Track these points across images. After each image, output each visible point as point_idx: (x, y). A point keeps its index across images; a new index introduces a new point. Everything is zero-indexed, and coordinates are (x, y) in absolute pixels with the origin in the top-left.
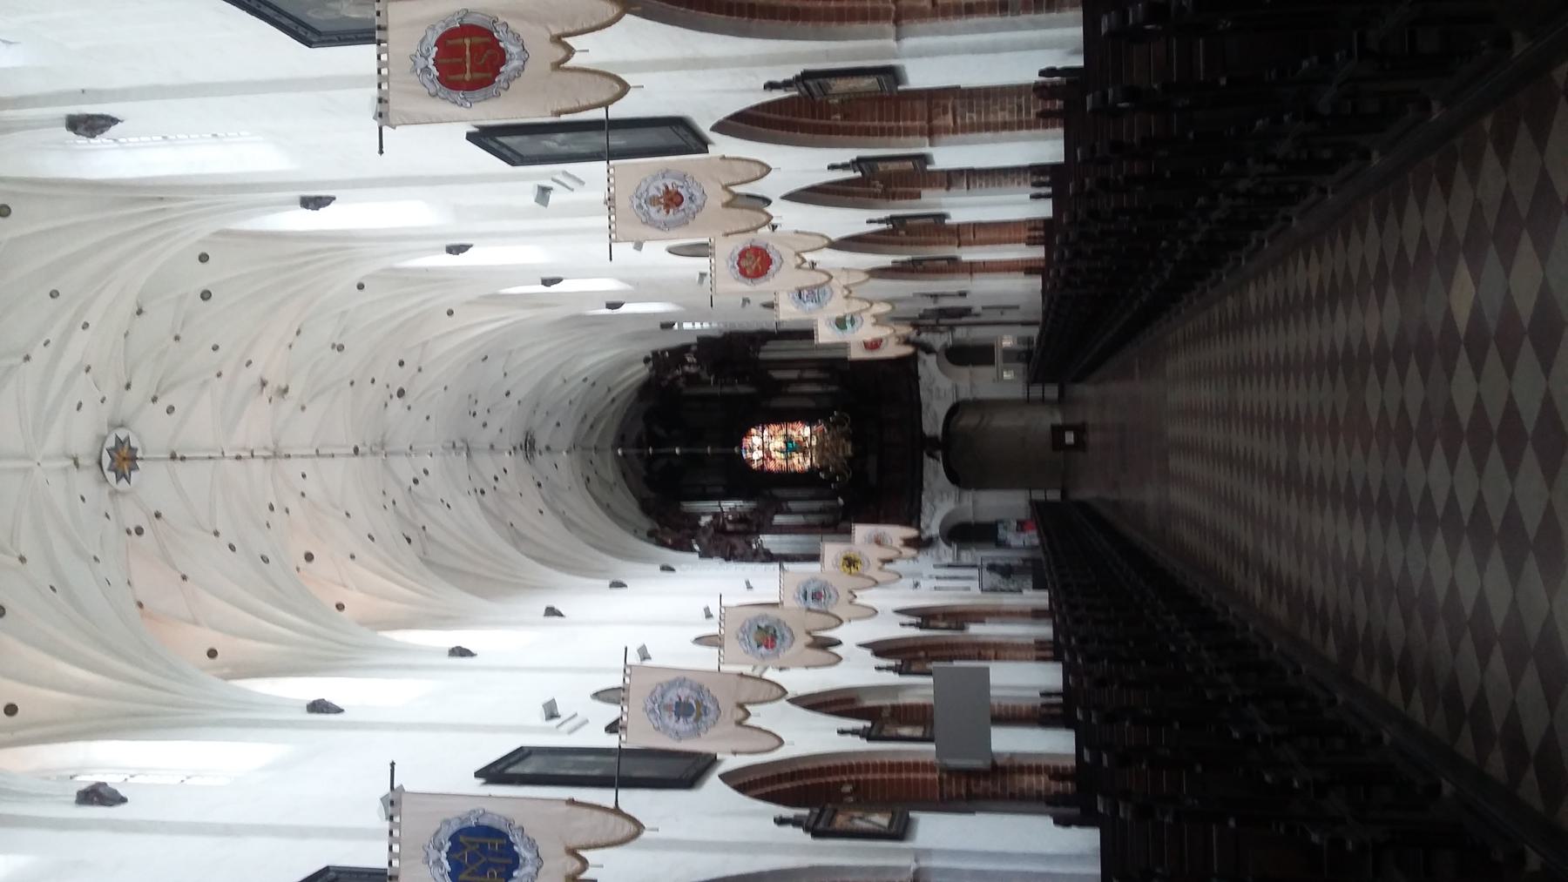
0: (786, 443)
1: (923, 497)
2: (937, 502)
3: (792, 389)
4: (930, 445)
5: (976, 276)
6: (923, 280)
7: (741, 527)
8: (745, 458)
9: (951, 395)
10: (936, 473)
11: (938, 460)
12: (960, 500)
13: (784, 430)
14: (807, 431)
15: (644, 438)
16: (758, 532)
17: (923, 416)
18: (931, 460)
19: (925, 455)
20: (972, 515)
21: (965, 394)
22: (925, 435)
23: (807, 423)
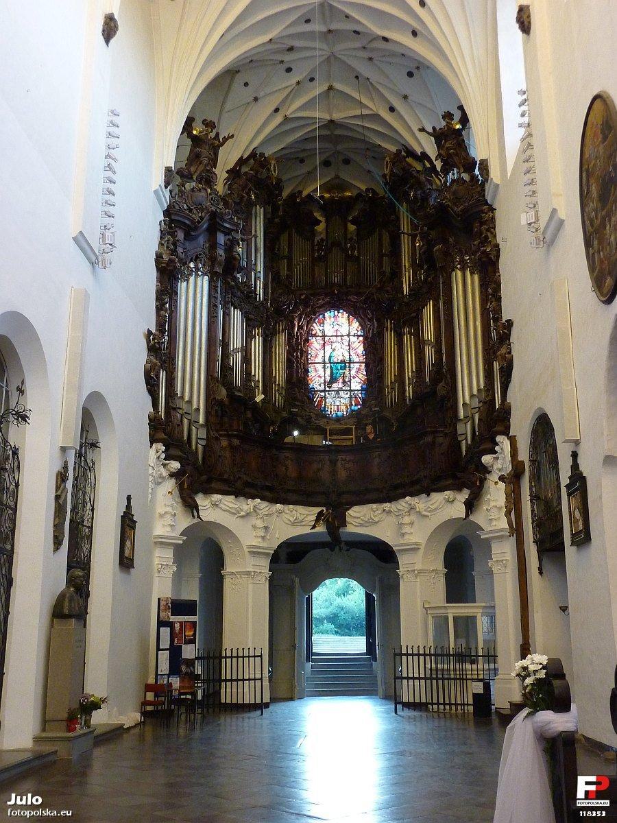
0: (343, 362)
1: (258, 501)
3: (408, 341)
4: (335, 520)
8: (327, 315)
9: (402, 542)
10: (294, 524)
11: (314, 527)
12: (255, 553)
13: (356, 360)
14: (356, 385)
15: (348, 194)
17: (374, 506)
19: (318, 509)
20: (234, 571)
21: (403, 560)
23: (365, 386)
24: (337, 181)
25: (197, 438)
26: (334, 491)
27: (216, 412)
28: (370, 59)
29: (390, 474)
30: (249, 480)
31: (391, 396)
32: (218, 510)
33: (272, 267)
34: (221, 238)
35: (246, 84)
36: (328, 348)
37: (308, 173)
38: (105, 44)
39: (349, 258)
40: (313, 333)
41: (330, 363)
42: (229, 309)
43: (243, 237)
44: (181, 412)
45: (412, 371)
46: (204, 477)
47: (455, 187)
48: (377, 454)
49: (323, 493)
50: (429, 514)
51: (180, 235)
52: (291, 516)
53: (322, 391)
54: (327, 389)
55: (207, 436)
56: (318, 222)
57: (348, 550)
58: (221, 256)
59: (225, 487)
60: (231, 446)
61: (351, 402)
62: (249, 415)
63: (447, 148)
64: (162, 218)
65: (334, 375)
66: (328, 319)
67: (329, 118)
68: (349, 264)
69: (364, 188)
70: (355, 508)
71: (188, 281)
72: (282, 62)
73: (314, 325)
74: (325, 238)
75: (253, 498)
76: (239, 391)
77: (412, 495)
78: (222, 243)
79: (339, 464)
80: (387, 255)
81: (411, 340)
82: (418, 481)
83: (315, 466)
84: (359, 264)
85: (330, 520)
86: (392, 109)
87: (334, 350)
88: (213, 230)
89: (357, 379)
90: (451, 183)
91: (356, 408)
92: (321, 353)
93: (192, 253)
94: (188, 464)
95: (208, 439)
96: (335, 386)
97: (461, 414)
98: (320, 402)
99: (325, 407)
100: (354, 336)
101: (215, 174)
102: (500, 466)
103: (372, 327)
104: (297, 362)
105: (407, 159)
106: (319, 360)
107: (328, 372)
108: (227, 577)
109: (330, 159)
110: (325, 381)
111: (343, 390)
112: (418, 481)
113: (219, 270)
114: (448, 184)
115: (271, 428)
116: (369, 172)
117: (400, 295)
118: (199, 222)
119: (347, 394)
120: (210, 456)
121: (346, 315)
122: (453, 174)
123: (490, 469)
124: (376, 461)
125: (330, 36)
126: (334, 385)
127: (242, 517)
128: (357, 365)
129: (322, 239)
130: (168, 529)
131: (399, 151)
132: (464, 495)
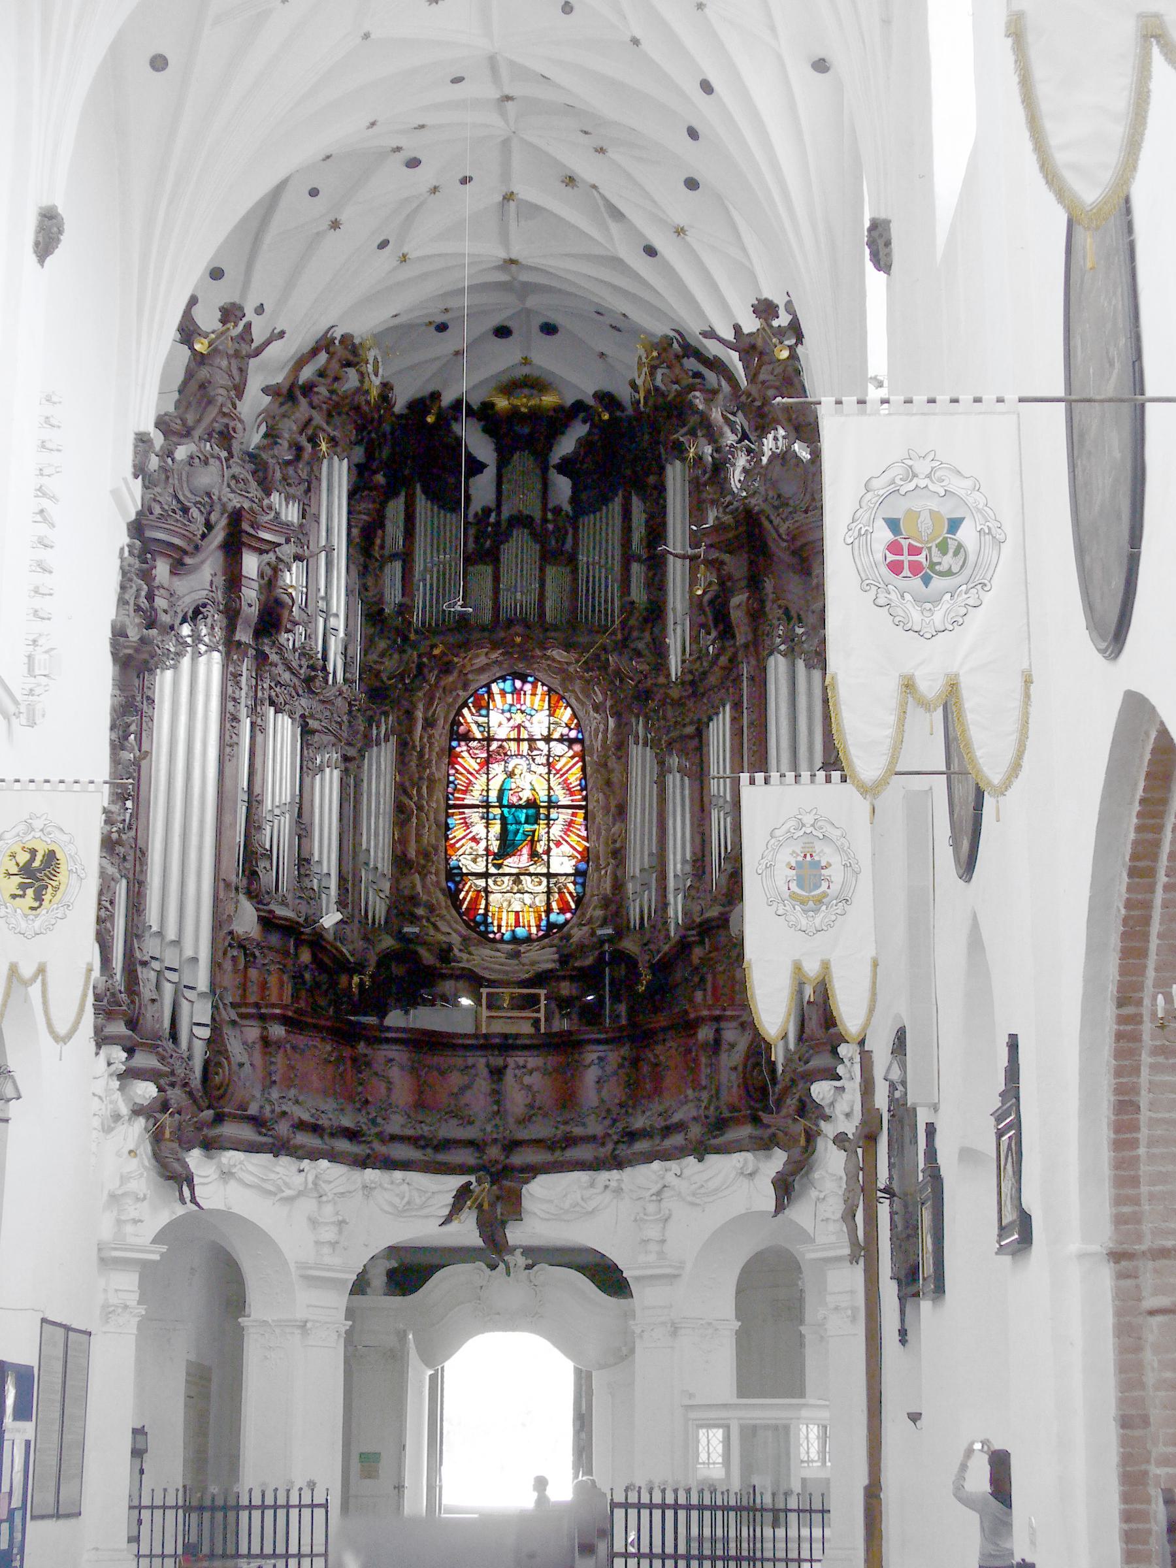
0: (532, 804)
1: (324, 1163)
2: (308, 1205)
5: (1105, 1276)
6: (1088, 1049)
7: (250, 594)
10: (405, 1211)
11: (448, 1220)
12: (312, 1281)
14: (562, 862)
15: (549, 400)
16: (231, 646)
17: (583, 1176)
18: (449, 1199)
19: (456, 1181)
22: (527, 1182)
24: (526, 370)
26: (495, 1141)
27: (234, 958)
28: (601, 150)
29: (621, 1105)
30: (306, 1117)
31: (638, 905)
32: (233, 1184)
33: (365, 588)
34: (251, 564)
35: (314, 193)
36: (497, 768)
38: (39, 266)
39: (547, 557)
40: (462, 729)
41: (501, 806)
42: (263, 716)
43: (300, 551)
44: (156, 965)
45: (684, 861)
46: (208, 1114)
47: (777, 471)
48: (594, 1056)
49: (471, 1143)
50: (698, 1201)
51: (162, 569)
52: (397, 1195)
53: (479, 875)
54: (492, 870)
55: (213, 1019)
56: (476, 467)
57: (529, 1267)
58: (250, 605)
59: (246, 1132)
60: (265, 1041)
61: (548, 904)
62: (305, 956)
63: (763, 382)
64: (124, 539)
65: (510, 837)
66: (497, 697)
67: (503, 255)
68: (551, 571)
70: (542, 1179)
71: (175, 668)
72: (398, 149)
73: (465, 711)
74: (493, 505)
75: (314, 1156)
76: (284, 903)
77: (665, 1156)
78: (255, 576)
80: (638, 559)
81: (683, 789)
82: (681, 1127)
83: (456, 1079)
84: (575, 571)
85: (486, 1206)
86: (651, 251)
87: (511, 775)
88: (233, 548)
89: (565, 848)
90: (770, 461)
91: (561, 919)
92: (480, 783)
93: (187, 603)
94: (173, 1085)
95: (216, 1025)
96: (513, 864)
98: (475, 902)
99: (485, 915)
100: (561, 740)
101: (241, 421)
102: (847, 1110)
103: (602, 727)
104: (420, 808)
105: (685, 361)
106: (474, 798)
107: (496, 828)
108: (251, 1330)
109: (509, 324)
110: (487, 849)
111: (530, 875)
112: (681, 1127)
113: (244, 635)
114: (765, 460)
115: (356, 979)
116: (602, 355)
117: (662, 680)
118: (204, 536)
119: (540, 883)
120: (219, 1064)
121: (540, 689)
122: (776, 439)
123: (827, 1111)
124: (591, 1075)
125: (509, 104)
126: (509, 861)
127: (290, 1200)
128: (566, 815)
129: (487, 511)
130: (129, 1229)
131: (667, 339)
132: (778, 1160)
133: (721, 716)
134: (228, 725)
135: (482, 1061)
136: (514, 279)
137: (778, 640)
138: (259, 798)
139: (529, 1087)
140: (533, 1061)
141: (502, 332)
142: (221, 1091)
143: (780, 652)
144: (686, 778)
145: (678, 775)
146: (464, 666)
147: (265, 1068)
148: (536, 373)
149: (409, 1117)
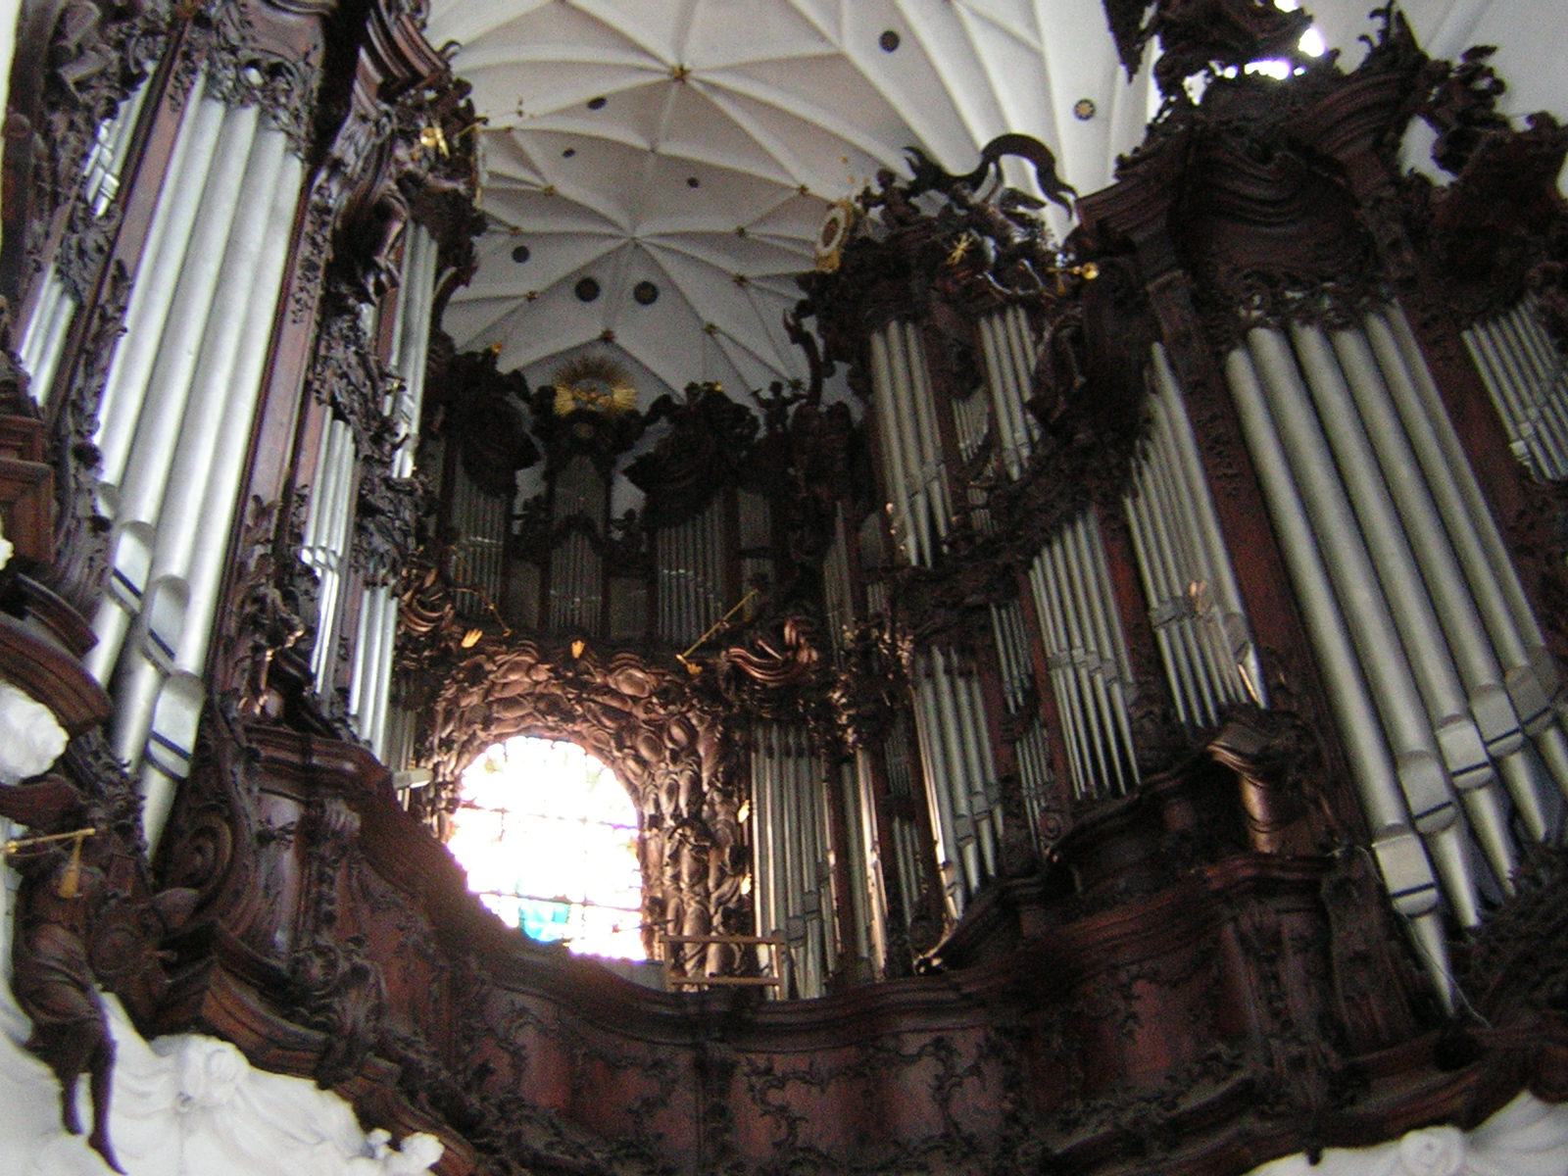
0: (564, 900)
24: (600, 352)
25: (151, 735)
29: (1012, 1118)
37: (531, 297)
45: (971, 792)
47: (1226, 96)
48: (927, 1038)
58: (364, 119)
60: (310, 833)
67: (672, 60)
68: (617, 587)
69: (679, 387)
79: (740, 1083)
80: (755, 553)
95: (204, 754)
97: (1386, 809)
105: (914, 200)
116: (711, 329)
133: (1057, 549)
134: (298, 272)
135: (684, 1059)
136: (653, 151)
137: (1256, 314)
138: (306, 491)
139: (783, 1110)
140: (781, 1064)
141: (587, 290)
142: (209, 887)
143: (1265, 325)
144: (961, 684)
145: (943, 682)
146: (493, 684)
147: (304, 891)
148: (615, 356)
149: (558, 1134)
